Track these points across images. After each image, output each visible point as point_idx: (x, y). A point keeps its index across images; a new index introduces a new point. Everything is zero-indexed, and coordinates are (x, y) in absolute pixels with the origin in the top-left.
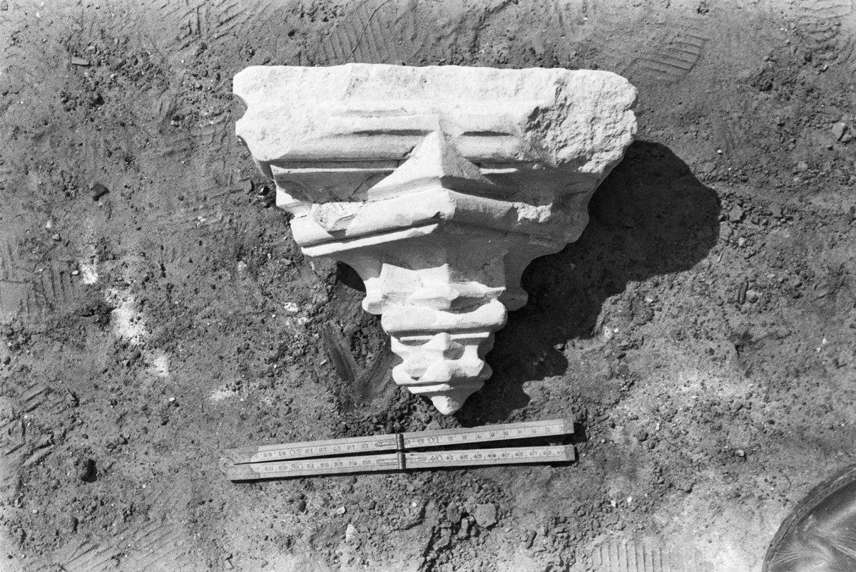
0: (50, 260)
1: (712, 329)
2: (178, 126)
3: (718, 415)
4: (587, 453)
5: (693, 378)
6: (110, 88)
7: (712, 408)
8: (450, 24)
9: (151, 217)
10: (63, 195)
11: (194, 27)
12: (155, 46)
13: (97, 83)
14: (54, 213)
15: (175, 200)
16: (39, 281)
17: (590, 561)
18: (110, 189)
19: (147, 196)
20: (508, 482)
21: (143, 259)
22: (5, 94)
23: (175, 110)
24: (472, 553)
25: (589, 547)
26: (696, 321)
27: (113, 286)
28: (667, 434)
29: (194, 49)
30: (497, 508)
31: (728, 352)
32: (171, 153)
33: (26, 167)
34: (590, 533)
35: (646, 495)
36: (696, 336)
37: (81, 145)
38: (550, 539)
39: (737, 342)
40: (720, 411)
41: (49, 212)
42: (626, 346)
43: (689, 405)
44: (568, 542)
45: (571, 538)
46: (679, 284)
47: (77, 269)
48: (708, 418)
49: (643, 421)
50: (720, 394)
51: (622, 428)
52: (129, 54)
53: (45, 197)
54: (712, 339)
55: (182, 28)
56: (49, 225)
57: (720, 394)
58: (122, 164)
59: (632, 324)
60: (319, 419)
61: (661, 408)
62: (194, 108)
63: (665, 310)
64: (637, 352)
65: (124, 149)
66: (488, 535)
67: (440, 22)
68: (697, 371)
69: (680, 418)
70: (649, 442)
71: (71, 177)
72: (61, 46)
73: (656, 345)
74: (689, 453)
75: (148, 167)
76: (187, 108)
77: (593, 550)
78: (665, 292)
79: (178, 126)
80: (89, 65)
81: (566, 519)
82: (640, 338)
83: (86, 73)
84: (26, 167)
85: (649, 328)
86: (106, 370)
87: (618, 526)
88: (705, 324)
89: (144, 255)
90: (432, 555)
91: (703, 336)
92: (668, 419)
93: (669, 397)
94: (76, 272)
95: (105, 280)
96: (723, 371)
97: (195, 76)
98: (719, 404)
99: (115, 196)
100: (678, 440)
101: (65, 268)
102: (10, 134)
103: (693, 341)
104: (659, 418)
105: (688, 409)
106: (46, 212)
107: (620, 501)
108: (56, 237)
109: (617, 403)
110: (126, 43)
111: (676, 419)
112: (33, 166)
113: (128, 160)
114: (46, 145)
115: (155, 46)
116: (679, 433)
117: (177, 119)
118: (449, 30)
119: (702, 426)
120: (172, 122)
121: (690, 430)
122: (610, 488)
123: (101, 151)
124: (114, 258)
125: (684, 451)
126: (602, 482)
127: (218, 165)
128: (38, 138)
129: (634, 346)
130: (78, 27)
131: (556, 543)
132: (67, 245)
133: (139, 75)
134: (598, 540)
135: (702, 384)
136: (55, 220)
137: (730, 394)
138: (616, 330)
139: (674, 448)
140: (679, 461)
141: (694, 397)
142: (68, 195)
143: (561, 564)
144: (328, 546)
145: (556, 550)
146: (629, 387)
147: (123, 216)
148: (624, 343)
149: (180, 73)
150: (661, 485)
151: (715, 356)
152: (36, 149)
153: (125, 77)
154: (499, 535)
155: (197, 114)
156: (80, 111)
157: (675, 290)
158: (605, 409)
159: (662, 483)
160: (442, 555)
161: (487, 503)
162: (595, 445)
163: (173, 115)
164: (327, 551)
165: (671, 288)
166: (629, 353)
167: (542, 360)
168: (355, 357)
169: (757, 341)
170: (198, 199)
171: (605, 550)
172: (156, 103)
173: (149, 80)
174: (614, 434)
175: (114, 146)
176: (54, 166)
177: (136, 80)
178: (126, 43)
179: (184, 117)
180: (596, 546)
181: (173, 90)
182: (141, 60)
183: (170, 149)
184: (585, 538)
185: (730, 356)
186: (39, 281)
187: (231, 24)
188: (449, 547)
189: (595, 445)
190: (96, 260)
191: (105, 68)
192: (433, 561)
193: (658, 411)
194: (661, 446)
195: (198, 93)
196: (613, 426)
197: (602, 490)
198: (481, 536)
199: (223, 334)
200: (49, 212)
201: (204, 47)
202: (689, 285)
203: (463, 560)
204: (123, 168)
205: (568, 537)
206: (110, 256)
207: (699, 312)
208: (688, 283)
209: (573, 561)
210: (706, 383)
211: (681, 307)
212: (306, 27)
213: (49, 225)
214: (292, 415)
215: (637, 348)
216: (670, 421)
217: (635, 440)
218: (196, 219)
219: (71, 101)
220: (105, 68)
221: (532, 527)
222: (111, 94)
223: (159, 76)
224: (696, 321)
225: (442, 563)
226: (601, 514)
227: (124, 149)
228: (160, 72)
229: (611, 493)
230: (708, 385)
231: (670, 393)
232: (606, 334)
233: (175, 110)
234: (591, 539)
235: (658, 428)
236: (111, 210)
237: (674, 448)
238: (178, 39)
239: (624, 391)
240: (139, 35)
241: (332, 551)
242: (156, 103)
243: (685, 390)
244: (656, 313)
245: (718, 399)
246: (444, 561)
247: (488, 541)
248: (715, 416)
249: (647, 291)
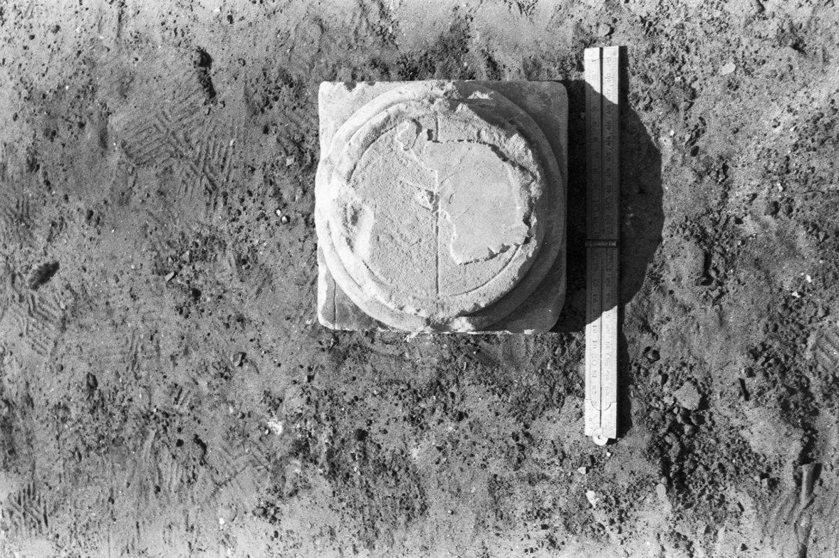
0: (248, 436)
1: (756, 52)
2: (249, 267)
3: (829, 126)
4: (734, 267)
5: (777, 113)
6: (197, 278)
7: (818, 124)
8: (354, 15)
9: (281, 349)
10: (223, 380)
11: (210, 187)
12: (199, 222)
13: (188, 282)
14: (229, 399)
15: (286, 324)
16: (253, 458)
17: (820, 368)
18: (244, 350)
19: (268, 335)
20: (686, 350)
21: (297, 385)
22: (152, 339)
23: (240, 256)
24: (713, 441)
25: (808, 355)
26: (736, 59)
27: (293, 423)
28: (794, 186)
29: (220, 200)
30: (695, 383)
31: (789, 59)
32: (259, 291)
33: (194, 380)
34: (798, 341)
35: (821, 262)
36: (748, 72)
37: (209, 334)
38: (760, 376)
39: (790, 42)
40: (826, 120)
41: (225, 401)
42: (690, 139)
43: (794, 141)
44: (783, 366)
45: (783, 360)
46: (692, 41)
47: (266, 428)
48: (822, 137)
49: (764, 193)
50: (816, 104)
51: (749, 217)
52: (190, 244)
53: (217, 391)
54: (764, 62)
55: (205, 194)
56: (231, 410)
57: (816, 104)
58: (238, 325)
59: (682, 114)
60: (497, 414)
61: (770, 168)
62: (250, 245)
63: (700, 75)
64: (706, 135)
65: (233, 315)
66: (711, 414)
67: (348, 21)
68: (774, 104)
69: (797, 160)
70: (783, 208)
71: (219, 363)
72: (156, 276)
73: (718, 112)
74: (832, 187)
75: (254, 315)
76: (246, 246)
77: (815, 355)
78: (687, 60)
79: (249, 267)
80: (176, 273)
81: (763, 344)
82: (699, 121)
83: (179, 281)
84: (194, 380)
85: (699, 107)
86: (334, 493)
87: (820, 314)
88: (746, 55)
89: (295, 382)
90: (674, 468)
91: (754, 67)
92: (784, 171)
93: (769, 150)
94: (267, 432)
95: (288, 421)
96: (799, 81)
97: (234, 220)
98: (822, 115)
99: (252, 353)
100: (810, 183)
101: (259, 433)
102: (171, 363)
103: (747, 79)
104: (775, 177)
105: (796, 146)
106: (223, 402)
107: (800, 288)
108: (240, 415)
109: (725, 196)
110: (183, 237)
111: (793, 165)
112: (195, 374)
113: (241, 319)
114: (194, 354)
115: (199, 222)
116: (807, 175)
117: (244, 262)
118: (357, 20)
119: (822, 150)
120: (243, 267)
121: (814, 163)
122: (782, 283)
123: (223, 328)
124: (281, 401)
125: (824, 189)
126: (770, 283)
127: (291, 271)
128: (186, 352)
129: (698, 133)
130: (155, 253)
131: (770, 375)
132: (249, 416)
133: (204, 252)
134: (811, 341)
135: (790, 110)
136: (232, 403)
137: (824, 95)
138: (672, 133)
139: (810, 194)
140: (826, 201)
141: (792, 129)
142: (226, 378)
143: (792, 391)
144: (586, 523)
145: (775, 382)
146: (725, 172)
147: (266, 365)
148: (687, 137)
149: (224, 227)
150: (827, 241)
151: (779, 74)
152: (190, 361)
153: (198, 262)
154: (719, 406)
155: (253, 246)
156: (193, 310)
157: (693, 49)
158: (719, 212)
159: (826, 237)
160: (687, 463)
161: (682, 384)
162: (736, 253)
163: (241, 261)
164: (590, 529)
165: (688, 50)
166: (700, 143)
167: (632, 215)
168: (486, 341)
169: (809, 23)
170: (297, 309)
171: (828, 346)
172: (225, 263)
173: (212, 250)
174: (746, 228)
175: (226, 316)
176: (206, 364)
177: (205, 257)
178: (183, 237)
179: (248, 258)
180: (814, 349)
181: (230, 244)
182: (198, 241)
183: (256, 289)
184: (799, 349)
185: (794, 62)
186: (253, 458)
187: (228, 162)
188: (685, 451)
189: (736, 253)
190: (273, 412)
191: (185, 267)
192: (680, 474)
193: (769, 172)
194: (798, 203)
195: (244, 231)
196: (739, 221)
197: (775, 290)
198: (707, 419)
199: (383, 400)
200: (225, 401)
201: (225, 195)
202: (702, 33)
203: (710, 454)
204: (241, 328)
205: (778, 361)
206: (277, 402)
207: (732, 48)
208: (700, 33)
209: (804, 380)
210: (793, 107)
211: (711, 59)
212: (270, 116)
213: (231, 410)
214: (476, 427)
215: (703, 132)
216: (788, 172)
217: (769, 218)
218: (307, 326)
219: (184, 309)
220: (185, 267)
221: (737, 376)
222: (200, 282)
223: (216, 241)
224: (736, 59)
225: (691, 472)
226: (794, 314)
227: (233, 315)
228: (213, 238)
229: (787, 287)
230: (796, 106)
231: (768, 145)
232: (665, 144)
233: (240, 256)
234: (804, 346)
235: (781, 188)
236: (256, 367)
237: (810, 194)
238: (208, 204)
239: (723, 181)
240: (187, 224)
241: (593, 525)
242: (225, 263)
243: (778, 130)
244: (694, 86)
245: (817, 111)
246: (692, 467)
247: (716, 418)
248: (826, 130)
249: (671, 73)
